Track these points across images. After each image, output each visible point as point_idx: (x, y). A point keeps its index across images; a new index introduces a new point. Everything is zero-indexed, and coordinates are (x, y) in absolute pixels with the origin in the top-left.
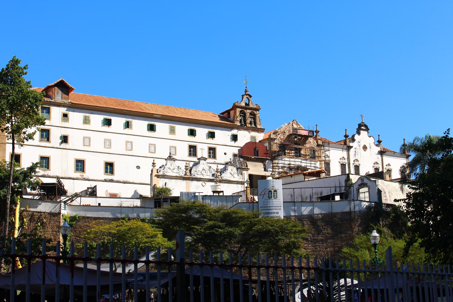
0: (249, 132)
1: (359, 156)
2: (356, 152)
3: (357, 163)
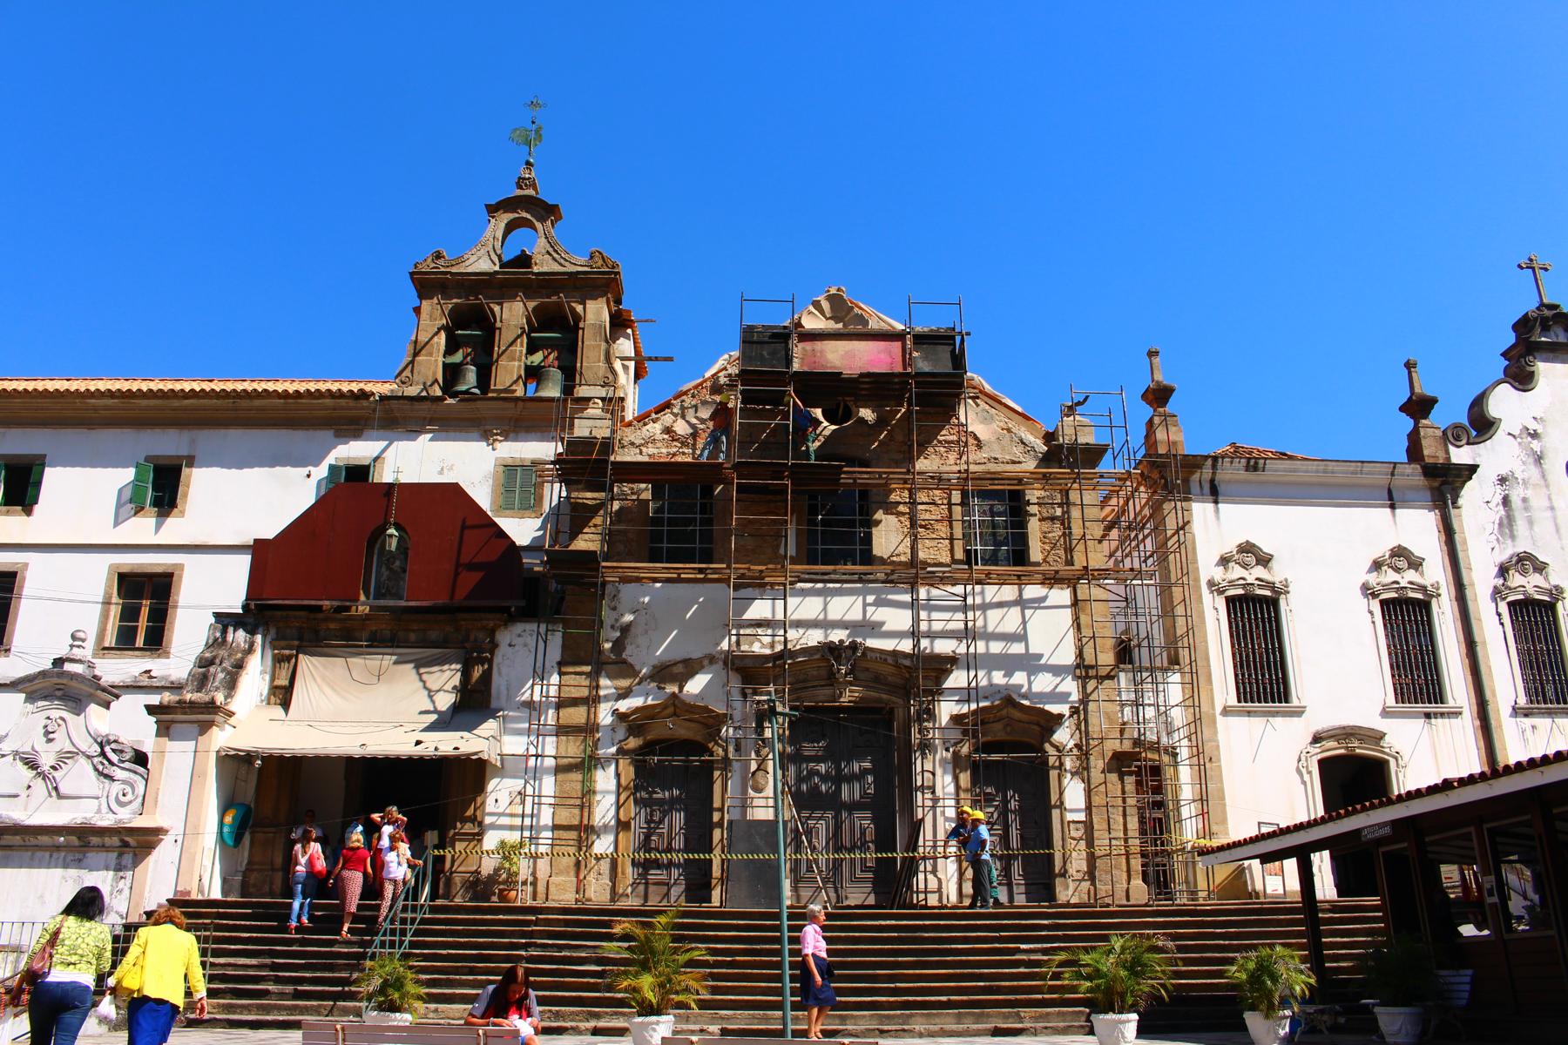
1: (1544, 526)
3: (1528, 584)
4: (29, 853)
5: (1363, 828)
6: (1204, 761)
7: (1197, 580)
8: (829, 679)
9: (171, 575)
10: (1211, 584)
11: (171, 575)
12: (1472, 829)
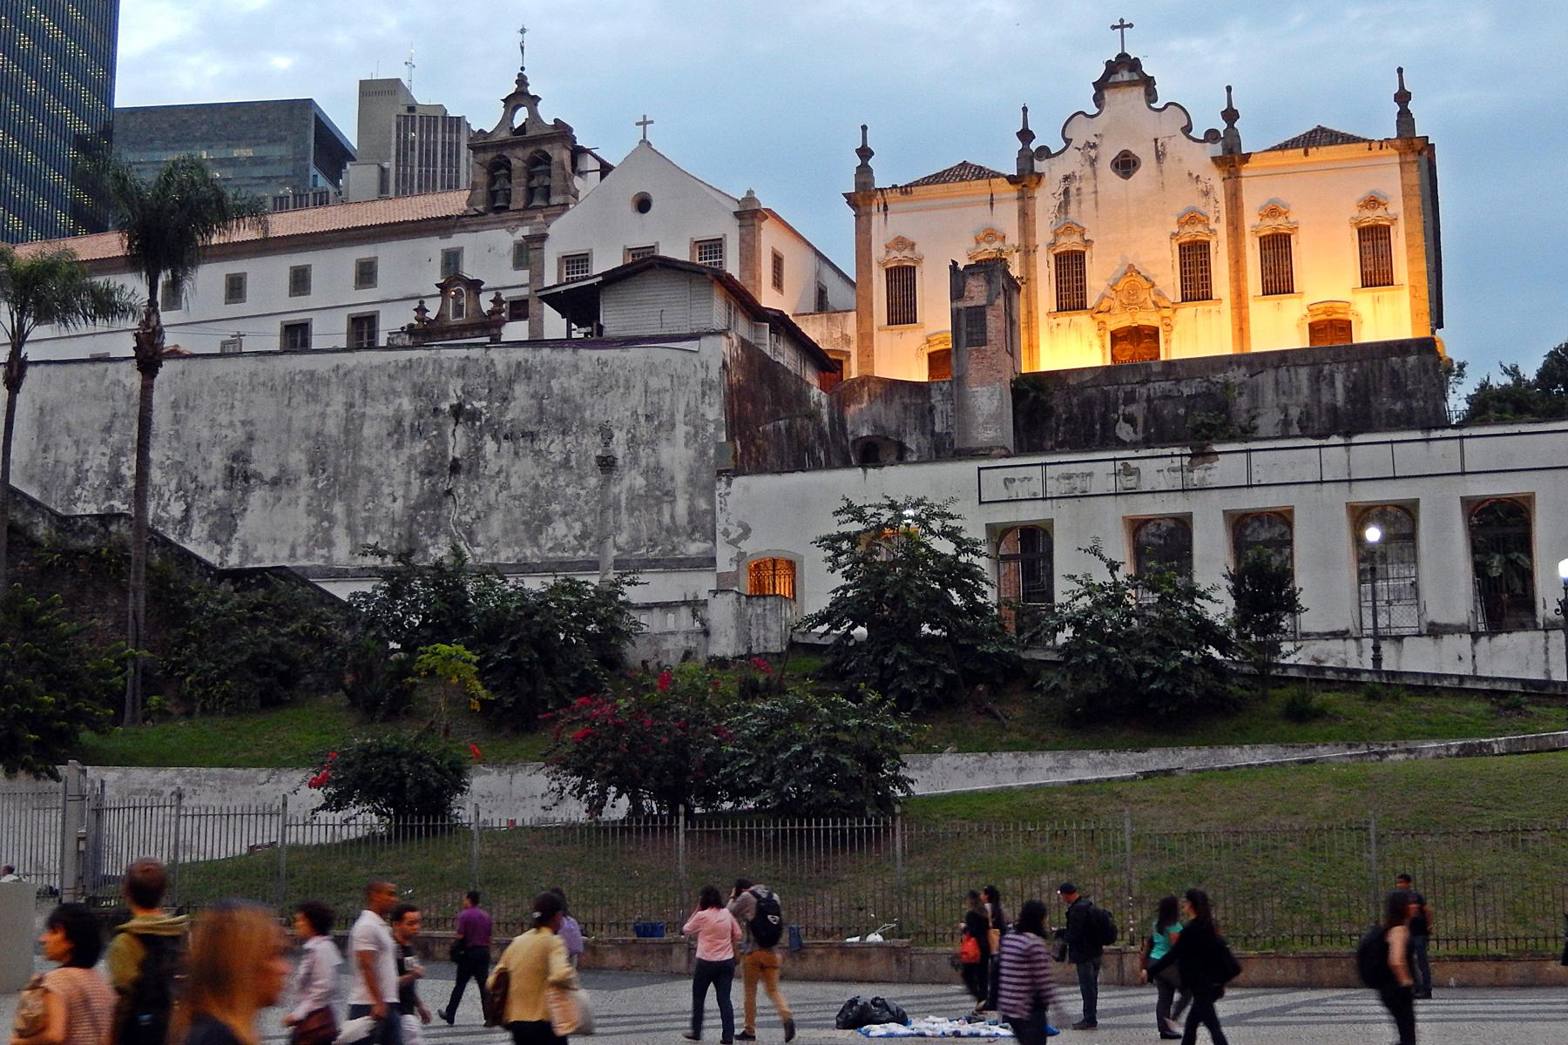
0: (512, 231)
1: (1088, 204)
2: (1073, 190)
7: (870, 260)
10: (881, 264)
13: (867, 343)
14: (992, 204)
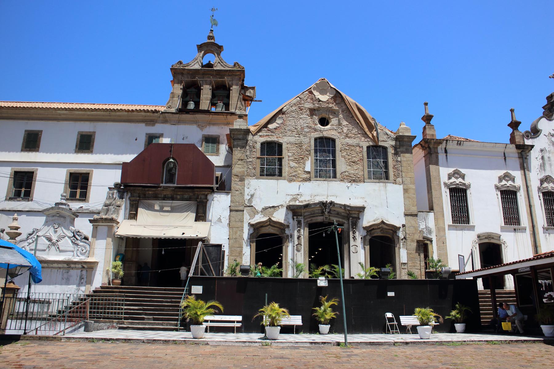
4: (50, 270)
5: (519, 268)
6: (442, 242)
7: (440, 182)
8: (322, 213)
9: (89, 174)
10: (445, 184)
11: (89, 174)
12: (550, 269)
13: (442, 234)
14: (505, 159)
